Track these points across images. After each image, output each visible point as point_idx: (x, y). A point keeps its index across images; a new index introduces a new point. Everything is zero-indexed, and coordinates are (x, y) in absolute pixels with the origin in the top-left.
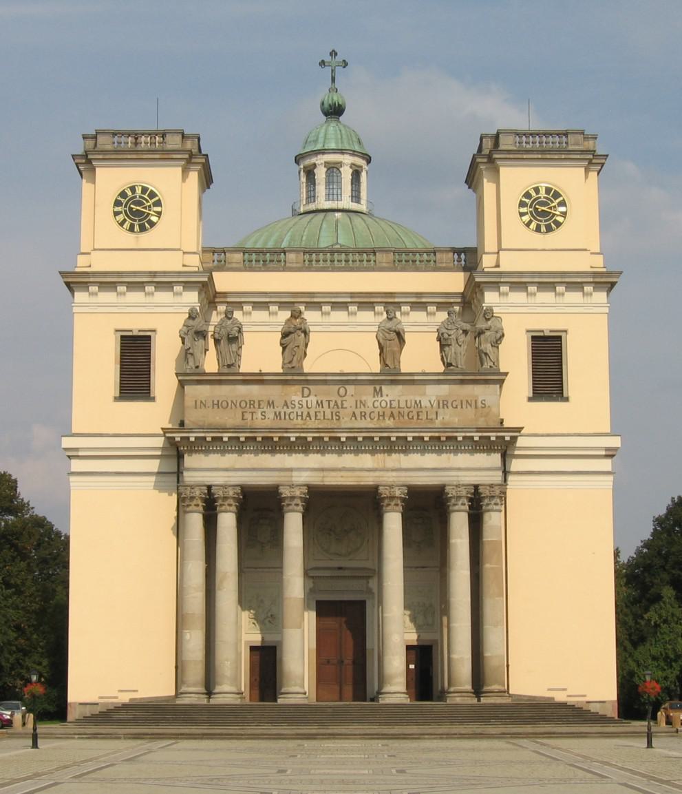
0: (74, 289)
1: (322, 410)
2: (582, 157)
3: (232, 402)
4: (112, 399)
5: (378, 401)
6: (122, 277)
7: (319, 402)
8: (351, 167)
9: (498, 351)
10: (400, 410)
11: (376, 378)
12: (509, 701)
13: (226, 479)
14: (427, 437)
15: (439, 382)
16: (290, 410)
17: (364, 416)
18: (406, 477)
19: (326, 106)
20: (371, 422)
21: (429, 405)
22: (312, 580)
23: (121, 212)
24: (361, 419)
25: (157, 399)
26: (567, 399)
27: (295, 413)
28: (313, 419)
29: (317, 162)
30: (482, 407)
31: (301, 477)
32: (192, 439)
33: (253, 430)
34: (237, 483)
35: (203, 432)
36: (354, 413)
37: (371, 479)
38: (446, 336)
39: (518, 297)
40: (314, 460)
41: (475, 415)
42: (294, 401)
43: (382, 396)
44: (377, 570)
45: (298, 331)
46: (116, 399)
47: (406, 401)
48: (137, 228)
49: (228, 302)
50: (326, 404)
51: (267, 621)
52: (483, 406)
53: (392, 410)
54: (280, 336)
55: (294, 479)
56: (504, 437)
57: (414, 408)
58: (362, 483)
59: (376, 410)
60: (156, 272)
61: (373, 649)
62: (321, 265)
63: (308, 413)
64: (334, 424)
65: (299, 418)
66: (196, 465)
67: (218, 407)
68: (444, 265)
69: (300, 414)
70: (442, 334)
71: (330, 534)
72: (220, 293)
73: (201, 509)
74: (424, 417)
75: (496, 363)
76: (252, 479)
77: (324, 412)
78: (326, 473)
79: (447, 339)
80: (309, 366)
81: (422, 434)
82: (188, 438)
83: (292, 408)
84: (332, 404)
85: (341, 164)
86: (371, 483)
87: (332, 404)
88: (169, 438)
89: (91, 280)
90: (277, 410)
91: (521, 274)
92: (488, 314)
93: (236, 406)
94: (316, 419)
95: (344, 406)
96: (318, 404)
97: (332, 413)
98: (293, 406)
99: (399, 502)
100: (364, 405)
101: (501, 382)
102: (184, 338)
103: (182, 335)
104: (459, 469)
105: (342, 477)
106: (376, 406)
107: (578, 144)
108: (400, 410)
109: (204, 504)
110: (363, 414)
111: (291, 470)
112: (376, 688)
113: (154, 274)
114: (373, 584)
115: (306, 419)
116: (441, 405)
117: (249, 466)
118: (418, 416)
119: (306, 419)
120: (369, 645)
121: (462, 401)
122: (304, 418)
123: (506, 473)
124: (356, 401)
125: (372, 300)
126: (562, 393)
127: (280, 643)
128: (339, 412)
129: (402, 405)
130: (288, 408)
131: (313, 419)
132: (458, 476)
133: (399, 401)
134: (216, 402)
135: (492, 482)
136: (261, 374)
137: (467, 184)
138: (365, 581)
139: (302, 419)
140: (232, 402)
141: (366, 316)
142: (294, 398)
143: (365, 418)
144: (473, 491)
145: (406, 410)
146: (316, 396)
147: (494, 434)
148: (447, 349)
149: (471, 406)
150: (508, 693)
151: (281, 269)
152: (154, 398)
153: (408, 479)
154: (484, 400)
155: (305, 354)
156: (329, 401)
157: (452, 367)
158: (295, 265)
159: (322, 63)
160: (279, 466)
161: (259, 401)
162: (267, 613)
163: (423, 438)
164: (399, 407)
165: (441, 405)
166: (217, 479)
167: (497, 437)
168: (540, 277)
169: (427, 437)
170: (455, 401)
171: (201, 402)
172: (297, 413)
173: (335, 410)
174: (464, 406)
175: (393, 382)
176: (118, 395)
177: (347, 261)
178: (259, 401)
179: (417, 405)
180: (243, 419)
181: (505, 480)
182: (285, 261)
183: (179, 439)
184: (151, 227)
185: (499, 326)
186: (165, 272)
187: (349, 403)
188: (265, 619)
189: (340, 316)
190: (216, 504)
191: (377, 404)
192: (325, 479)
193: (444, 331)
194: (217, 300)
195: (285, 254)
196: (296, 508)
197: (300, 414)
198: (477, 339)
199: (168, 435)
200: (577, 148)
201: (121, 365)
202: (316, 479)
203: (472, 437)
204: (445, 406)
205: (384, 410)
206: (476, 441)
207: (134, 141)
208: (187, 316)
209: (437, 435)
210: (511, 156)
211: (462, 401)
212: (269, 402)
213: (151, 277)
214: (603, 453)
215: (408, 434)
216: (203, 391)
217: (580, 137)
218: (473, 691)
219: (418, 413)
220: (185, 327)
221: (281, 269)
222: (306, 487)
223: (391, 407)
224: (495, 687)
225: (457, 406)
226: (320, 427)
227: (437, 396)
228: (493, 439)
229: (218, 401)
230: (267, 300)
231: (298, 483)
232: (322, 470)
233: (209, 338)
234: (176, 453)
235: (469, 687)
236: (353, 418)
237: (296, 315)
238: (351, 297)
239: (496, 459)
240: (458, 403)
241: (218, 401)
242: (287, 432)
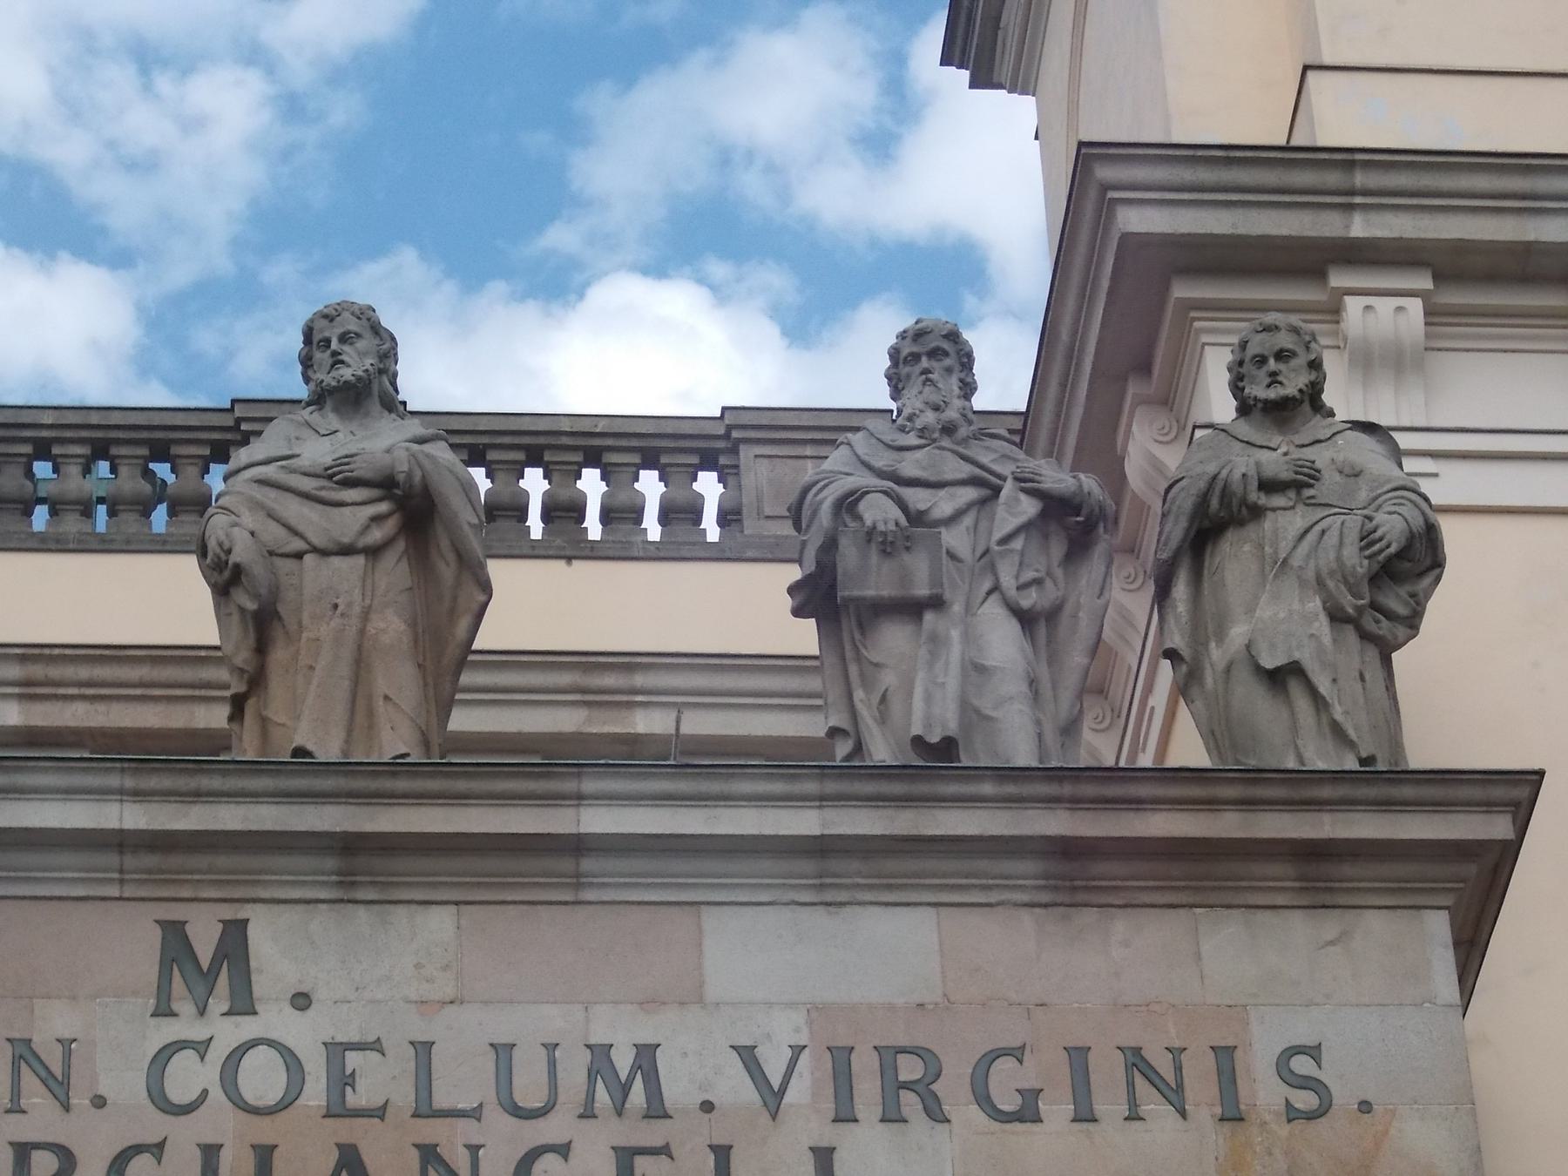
5: (202, 1048)
10: (431, 1131)
21: (735, 1088)
43: (243, 1006)
47: (503, 1052)
52: (1305, 1100)
53: (346, 1131)
57: (588, 1113)
100: (59, 1088)
108: (431, 1131)
116: (867, 1089)
121: (1078, 1057)
133: (424, 1050)
149: (1175, 1096)
154: (1314, 1052)
164: (425, 1111)
165: (867, 1089)
170: (1017, 1053)
174: (1110, 1105)
204: (910, 1102)
205: (264, 1132)
211: (1078, 1057)
223: (336, 1110)
225: (1031, 1096)
227: (817, 1012)
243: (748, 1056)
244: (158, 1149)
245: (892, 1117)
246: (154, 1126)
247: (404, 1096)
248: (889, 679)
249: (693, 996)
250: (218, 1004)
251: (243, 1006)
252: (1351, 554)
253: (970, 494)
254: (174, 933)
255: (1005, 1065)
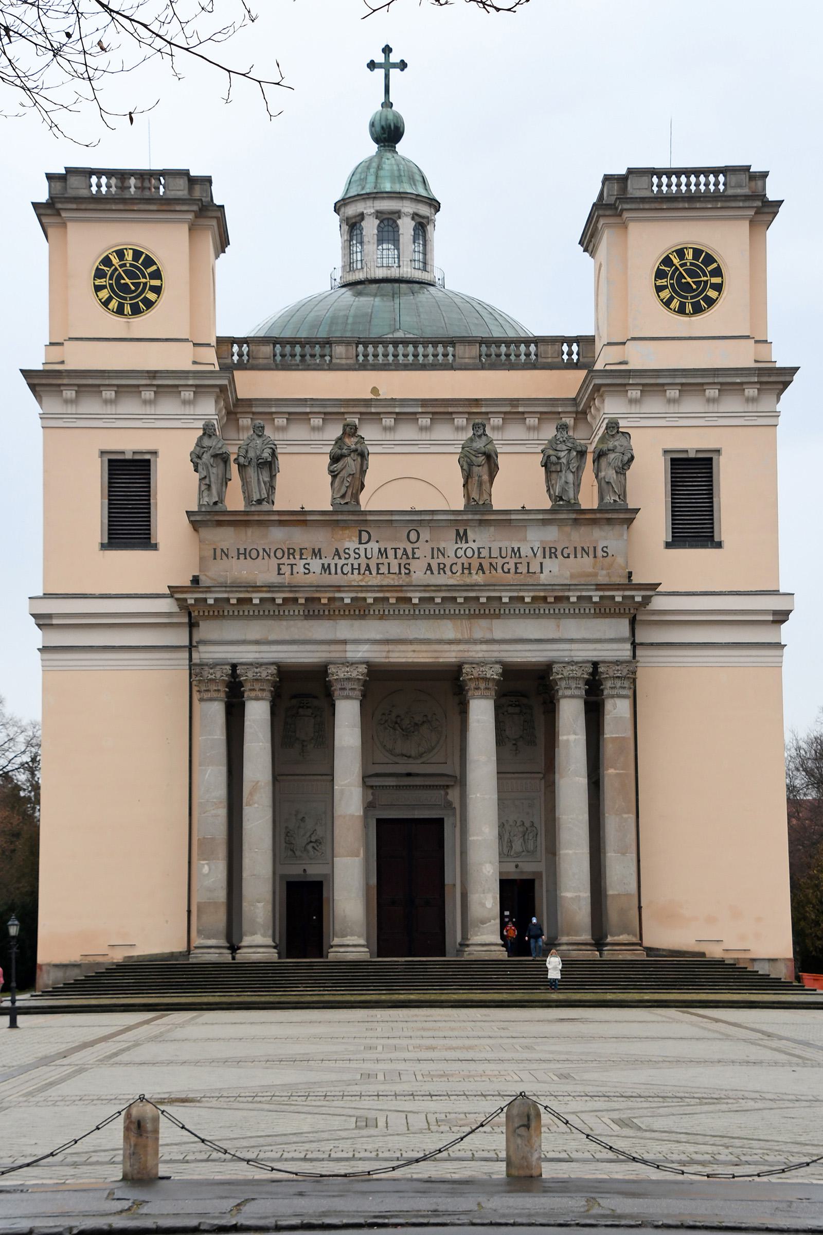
0: (41, 393)
1: (386, 561)
2: (747, 204)
3: (264, 550)
4: (97, 546)
5: (461, 548)
6: (109, 378)
7: (383, 550)
8: (413, 219)
9: (625, 479)
10: (491, 560)
11: (460, 518)
12: (642, 956)
13: (257, 655)
14: (529, 597)
15: (545, 522)
16: (343, 561)
17: (443, 569)
18: (500, 651)
19: (378, 128)
20: (451, 578)
22: (370, 792)
23: (104, 287)
24: (439, 573)
25: (161, 546)
26: (719, 545)
27: (350, 565)
28: (374, 572)
29: (365, 212)
30: (603, 557)
31: (359, 651)
32: (211, 601)
33: (292, 588)
34: (272, 660)
35: (226, 592)
36: (429, 565)
37: (454, 654)
38: (553, 459)
39: (654, 405)
40: (373, 629)
41: (593, 568)
42: (349, 549)
43: (467, 542)
44: (458, 778)
45: (352, 455)
46: (103, 547)
47: (500, 548)
48: (127, 309)
49: (253, 413)
50: (391, 553)
51: (309, 847)
52: (605, 554)
53: (480, 560)
54: (327, 460)
55: (349, 655)
56: (633, 597)
58: (441, 660)
59: (459, 561)
60: (156, 372)
61: (454, 885)
62: (381, 362)
63: (368, 565)
64: (402, 580)
65: (356, 572)
66: (214, 636)
67: (246, 558)
68: (549, 360)
69: (356, 566)
70: (549, 457)
71: (394, 729)
72: (242, 400)
73: (222, 695)
74: (525, 571)
75: (623, 495)
76: (292, 655)
77: (389, 564)
78: (391, 647)
79: (557, 463)
80: (369, 501)
81: (521, 594)
82: (205, 600)
83: (345, 558)
84: (400, 553)
85: (398, 214)
86: (454, 660)
87: (400, 553)
88: (177, 599)
89: (65, 381)
90: (326, 561)
91: (657, 373)
92: (613, 427)
93: (269, 556)
94: (378, 573)
95: (415, 556)
96: (383, 553)
97: (400, 564)
98: (347, 556)
99: (491, 685)
100: (443, 555)
101: (630, 521)
102: (197, 463)
103: (196, 460)
104: (571, 641)
105: (414, 651)
106: (459, 555)
107: (740, 186)
109: (227, 690)
110: (442, 566)
111: (344, 642)
112: (459, 939)
113: (153, 374)
114: (454, 795)
115: (364, 574)
117: (287, 637)
118: (516, 568)
119: (364, 574)
120: (448, 880)
121: (575, 548)
122: (362, 572)
123: (634, 645)
124: (433, 549)
125: (450, 410)
126: (713, 536)
127: (330, 876)
128: (409, 564)
129: (495, 553)
130: (340, 558)
131: (374, 572)
132: (571, 650)
133: (490, 548)
134: (242, 551)
135: (616, 658)
136: (303, 512)
137: (582, 246)
138: (442, 792)
139: (359, 573)
140: (264, 550)
141: (444, 432)
142: (347, 545)
143: (445, 573)
144: (591, 669)
145: (500, 561)
146: (377, 542)
147: (621, 593)
148: (554, 475)
149: (588, 554)
150: (641, 945)
151: (326, 367)
152: (156, 544)
153: (503, 654)
154: (607, 547)
155: (362, 486)
156: (395, 549)
157: (561, 503)
158: (344, 361)
159: (372, 65)
160: (330, 636)
161: (301, 549)
162: (310, 837)
163: (523, 598)
164: (490, 557)
166: (245, 654)
167: (624, 597)
168: (685, 376)
169: (529, 597)
171: (222, 550)
172: (352, 565)
173: (403, 562)
174: (579, 555)
175: (481, 522)
176: (106, 541)
177: (416, 356)
178: (301, 549)
179: (515, 554)
180: (279, 574)
181: (634, 656)
182: (331, 356)
183: (192, 602)
184: (148, 308)
185: (625, 444)
186: (167, 372)
187: (423, 550)
188: (308, 844)
189: (407, 432)
190: (242, 689)
191: (460, 553)
192: (391, 655)
193: (551, 452)
194: (239, 410)
195: (331, 347)
196: (351, 693)
197: (356, 566)
198: (596, 463)
199: (178, 596)
200: (739, 191)
201: (109, 500)
202: (377, 654)
203: (590, 597)
205: (470, 561)
206: (595, 603)
207: (120, 184)
208: (201, 432)
209: (542, 594)
210: (647, 206)
211: (575, 548)
212: (314, 550)
213: (149, 378)
214: (770, 618)
215: (503, 594)
216: (226, 538)
217: (744, 177)
218: (593, 942)
219: (516, 564)
220: (198, 448)
221: (326, 367)
222: (365, 666)
223: (479, 557)
224: (623, 938)
225: (569, 554)
226: (384, 583)
227: (542, 542)
228: (618, 599)
229: (245, 549)
230: (308, 410)
231: (354, 660)
232: (387, 642)
233: (232, 464)
234: (186, 620)
235: (586, 937)
236: (429, 572)
237: (351, 431)
238: (422, 406)
239: (622, 627)
240: (570, 551)
241: (245, 549)
242: (339, 591)
243: (532, 548)
244: (456, 564)
245: (551, 557)
246: (456, 560)
247: (488, 555)
248: (553, 482)
249: (525, 539)
250: (464, 542)
251: (467, 542)
252: (619, 463)
253: (567, 452)
254: (457, 531)
255: (566, 549)
